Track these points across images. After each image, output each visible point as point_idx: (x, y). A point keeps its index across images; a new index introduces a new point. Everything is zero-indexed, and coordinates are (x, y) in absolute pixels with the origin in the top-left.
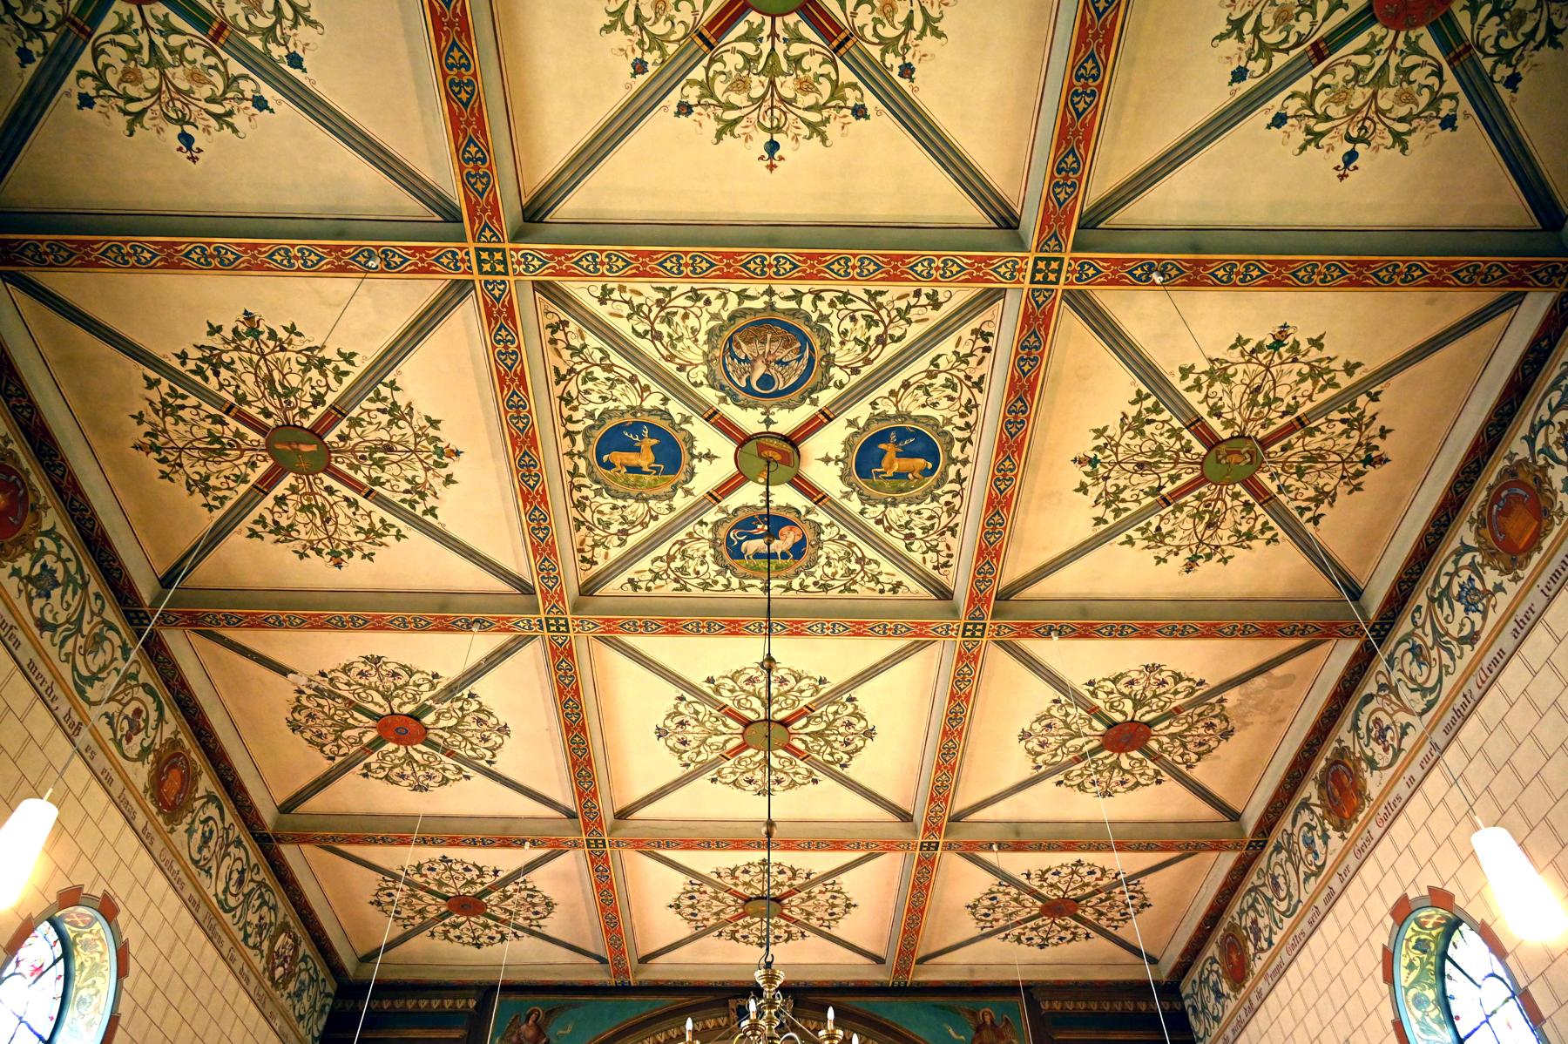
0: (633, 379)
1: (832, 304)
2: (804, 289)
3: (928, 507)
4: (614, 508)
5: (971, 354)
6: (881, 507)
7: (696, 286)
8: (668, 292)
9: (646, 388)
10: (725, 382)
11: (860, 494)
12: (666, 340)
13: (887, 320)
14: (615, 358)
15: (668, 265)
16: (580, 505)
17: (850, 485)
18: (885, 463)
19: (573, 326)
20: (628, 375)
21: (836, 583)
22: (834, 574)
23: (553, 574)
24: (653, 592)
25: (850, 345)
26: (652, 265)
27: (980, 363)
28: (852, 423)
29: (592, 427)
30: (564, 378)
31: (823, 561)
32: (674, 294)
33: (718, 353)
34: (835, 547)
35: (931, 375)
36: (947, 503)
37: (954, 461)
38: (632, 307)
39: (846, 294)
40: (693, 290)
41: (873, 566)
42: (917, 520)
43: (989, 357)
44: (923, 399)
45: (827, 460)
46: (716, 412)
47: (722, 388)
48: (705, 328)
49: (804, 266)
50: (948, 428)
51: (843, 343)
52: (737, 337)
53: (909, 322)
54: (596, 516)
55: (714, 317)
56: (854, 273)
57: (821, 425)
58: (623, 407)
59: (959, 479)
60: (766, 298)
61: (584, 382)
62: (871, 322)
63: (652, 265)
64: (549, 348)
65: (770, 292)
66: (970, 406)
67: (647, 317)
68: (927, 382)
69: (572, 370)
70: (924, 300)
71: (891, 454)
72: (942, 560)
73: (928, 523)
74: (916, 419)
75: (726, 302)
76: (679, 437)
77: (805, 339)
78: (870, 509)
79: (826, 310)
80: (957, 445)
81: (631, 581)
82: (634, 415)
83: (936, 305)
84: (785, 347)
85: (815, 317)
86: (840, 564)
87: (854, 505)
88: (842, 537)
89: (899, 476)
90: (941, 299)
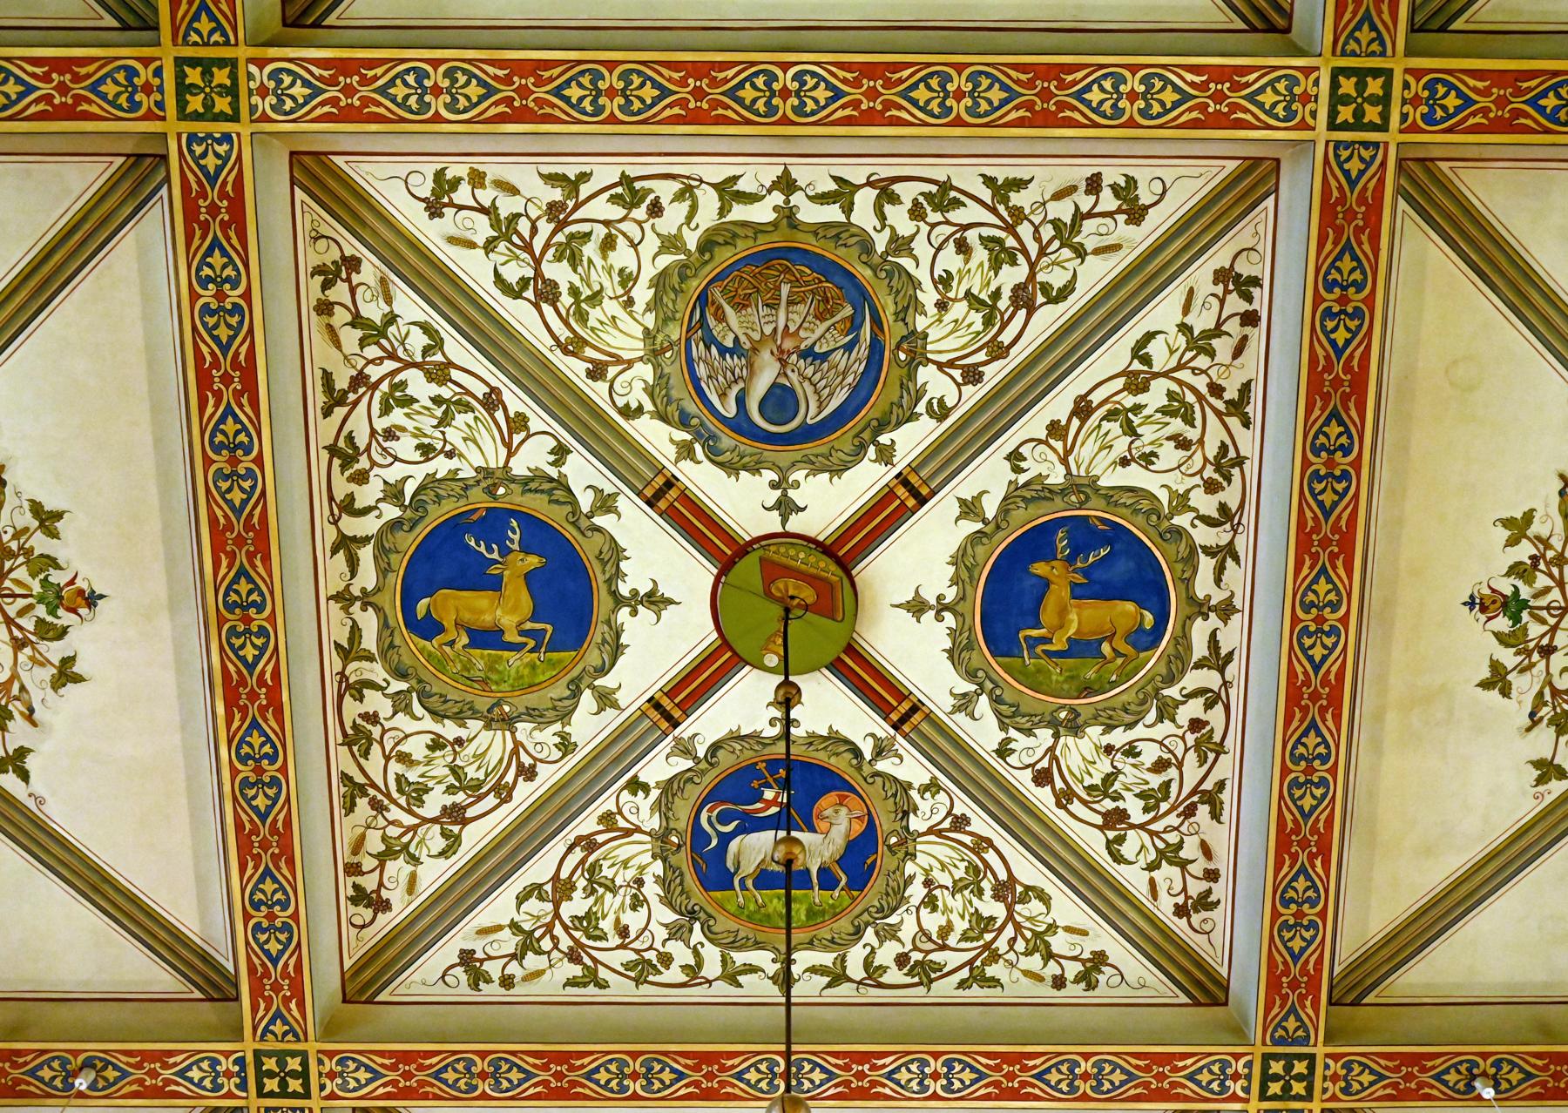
0: (492, 401)
1: (916, 213)
2: (857, 175)
3: (1152, 735)
4: (437, 744)
5: (1218, 331)
6: (1045, 736)
7: (633, 172)
8: (571, 185)
9: (519, 423)
10: (691, 407)
11: (996, 701)
12: (566, 300)
13: (1033, 249)
14: (457, 349)
15: (574, 92)
16: (358, 739)
17: (971, 675)
18: (1048, 614)
19: (370, 270)
20: (480, 390)
21: (951, 959)
22: (946, 930)
23: (283, 916)
24: (520, 991)
25: (959, 310)
26: (540, 93)
27: (1238, 352)
28: (969, 508)
29: (395, 525)
30: (341, 402)
31: (916, 892)
32: (585, 190)
33: (675, 332)
34: (943, 851)
35: (1137, 384)
36: (1196, 724)
37: (1201, 609)
38: (496, 224)
39: (946, 186)
40: (626, 180)
41: (1035, 906)
42: (1130, 774)
43: (1257, 335)
44: (1121, 446)
45: (917, 607)
46: (670, 483)
47: (684, 422)
48: (649, 272)
49: (855, 94)
50: (1182, 520)
51: (942, 306)
52: (716, 293)
53: (1081, 253)
54: (395, 767)
55: (670, 243)
56: (960, 108)
57: (901, 516)
58: (467, 473)
59: (1218, 660)
60: (777, 198)
61: (386, 410)
62: (1000, 256)
63: (540, 93)
64: (314, 322)
65: (786, 184)
66: (1227, 463)
67: (528, 247)
68: (1129, 401)
69: (359, 380)
70: (1108, 202)
71: (1059, 592)
72: (1196, 888)
73: (1155, 781)
74: (1111, 496)
75: (693, 209)
76: (588, 548)
77: (861, 297)
78: (1020, 741)
79: (905, 227)
80: (1206, 565)
81: (467, 958)
82: (491, 491)
83: (1136, 214)
84: (821, 317)
85: (880, 247)
86: (957, 903)
87: (983, 731)
88: (960, 823)
89: (1083, 648)
90: (1145, 198)
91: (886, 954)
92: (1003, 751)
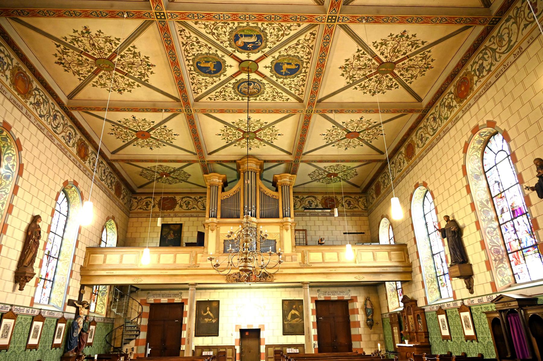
6: (211, 52)
11: (218, 56)
22: (222, 28)
31: (227, 34)
34: (224, 39)
36: (189, 53)
41: (208, 31)
42: (197, 48)
76: (274, 72)
78: (214, 52)
86: (221, 32)
87: (220, 53)
88: (222, 42)
91: (231, 25)
92: (216, 51)
